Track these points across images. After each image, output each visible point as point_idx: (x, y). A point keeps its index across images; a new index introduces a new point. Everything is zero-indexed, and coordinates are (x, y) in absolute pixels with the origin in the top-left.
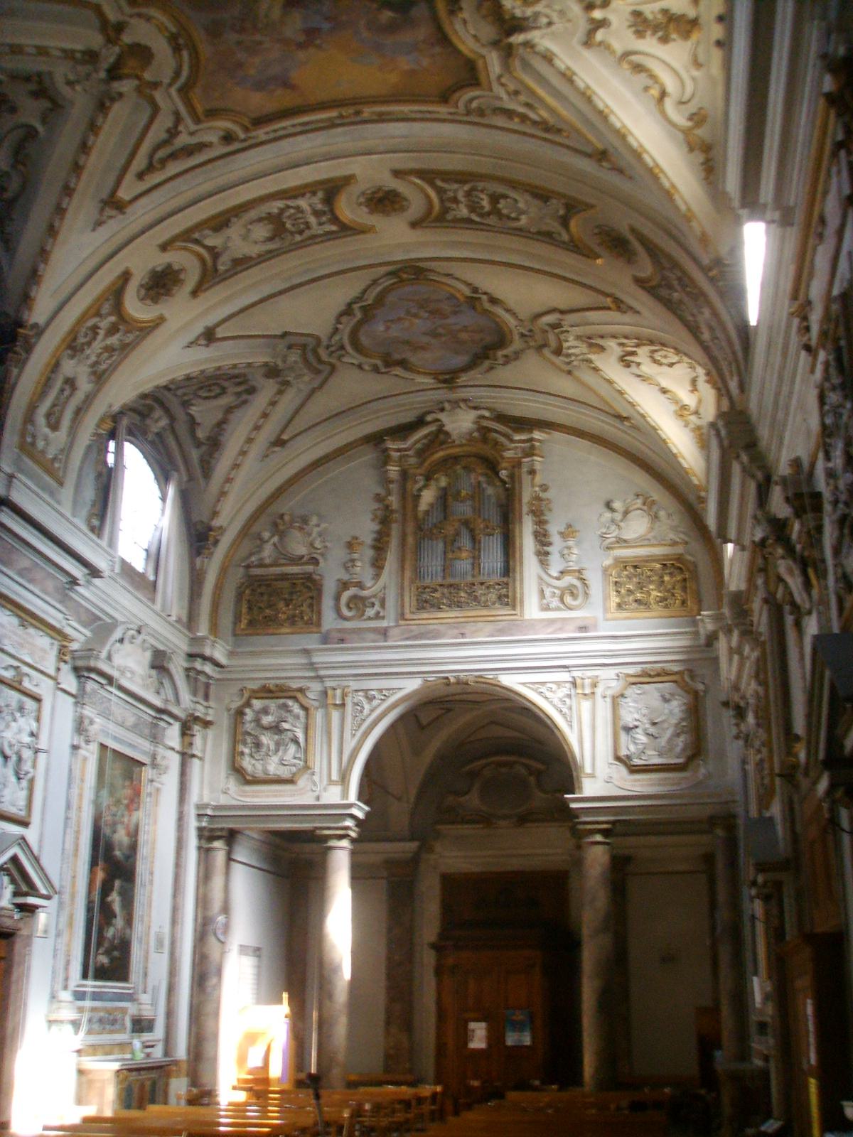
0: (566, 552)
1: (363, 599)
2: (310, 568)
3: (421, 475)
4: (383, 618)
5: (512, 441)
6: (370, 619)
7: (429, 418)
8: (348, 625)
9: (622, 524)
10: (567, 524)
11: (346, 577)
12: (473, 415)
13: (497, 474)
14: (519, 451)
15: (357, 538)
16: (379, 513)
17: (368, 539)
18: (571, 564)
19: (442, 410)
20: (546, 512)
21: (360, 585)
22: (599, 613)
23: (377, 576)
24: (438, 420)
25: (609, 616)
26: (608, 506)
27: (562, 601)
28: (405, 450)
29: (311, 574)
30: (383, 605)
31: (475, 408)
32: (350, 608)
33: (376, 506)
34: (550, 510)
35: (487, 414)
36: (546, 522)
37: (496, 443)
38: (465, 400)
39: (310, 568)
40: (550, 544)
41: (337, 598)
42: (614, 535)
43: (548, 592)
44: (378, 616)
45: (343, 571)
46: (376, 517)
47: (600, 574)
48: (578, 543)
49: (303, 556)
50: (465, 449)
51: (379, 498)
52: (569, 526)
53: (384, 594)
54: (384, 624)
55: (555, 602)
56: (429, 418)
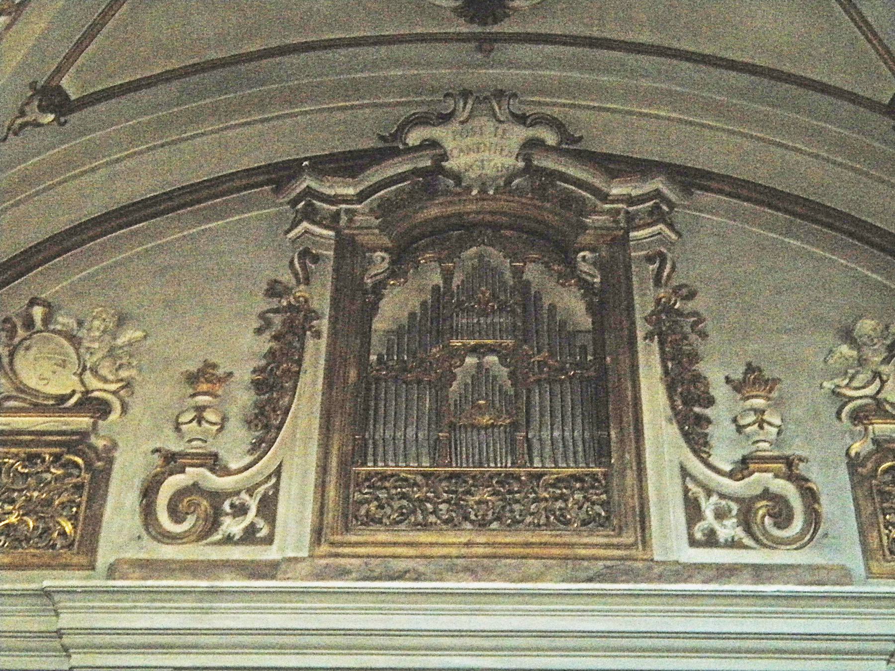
0: (751, 418)
1: (216, 497)
2: (83, 422)
3: (386, 250)
4: (269, 540)
5: (604, 197)
6: (228, 540)
7: (414, 137)
8: (168, 552)
9: (885, 369)
10: (749, 365)
11: (174, 446)
12: (519, 134)
13: (571, 264)
14: (621, 216)
15: (214, 366)
16: (277, 319)
17: (244, 374)
18: (762, 445)
19: (445, 119)
20: (693, 337)
21: (213, 462)
22: (854, 560)
23: (260, 447)
24: (433, 144)
25: (875, 567)
26: (848, 335)
27: (746, 523)
28: (345, 200)
29: (84, 435)
30: (268, 508)
31: (521, 119)
32: (176, 515)
33: (263, 304)
34: (703, 335)
35: (551, 139)
36: (694, 357)
37: (567, 201)
38: (499, 94)
39: (83, 422)
40: (710, 402)
41: (149, 492)
42: (871, 390)
43: (708, 507)
44: (250, 536)
45: (169, 431)
46: (268, 324)
47: (843, 475)
48: (778, 404)
49: (63, 399)
50: (488, 205)
51: (274, 290)
52: (750, 368)
53: (276, 487)
54: (272, 554)
55: (728, 530)
56: (414, 137)
